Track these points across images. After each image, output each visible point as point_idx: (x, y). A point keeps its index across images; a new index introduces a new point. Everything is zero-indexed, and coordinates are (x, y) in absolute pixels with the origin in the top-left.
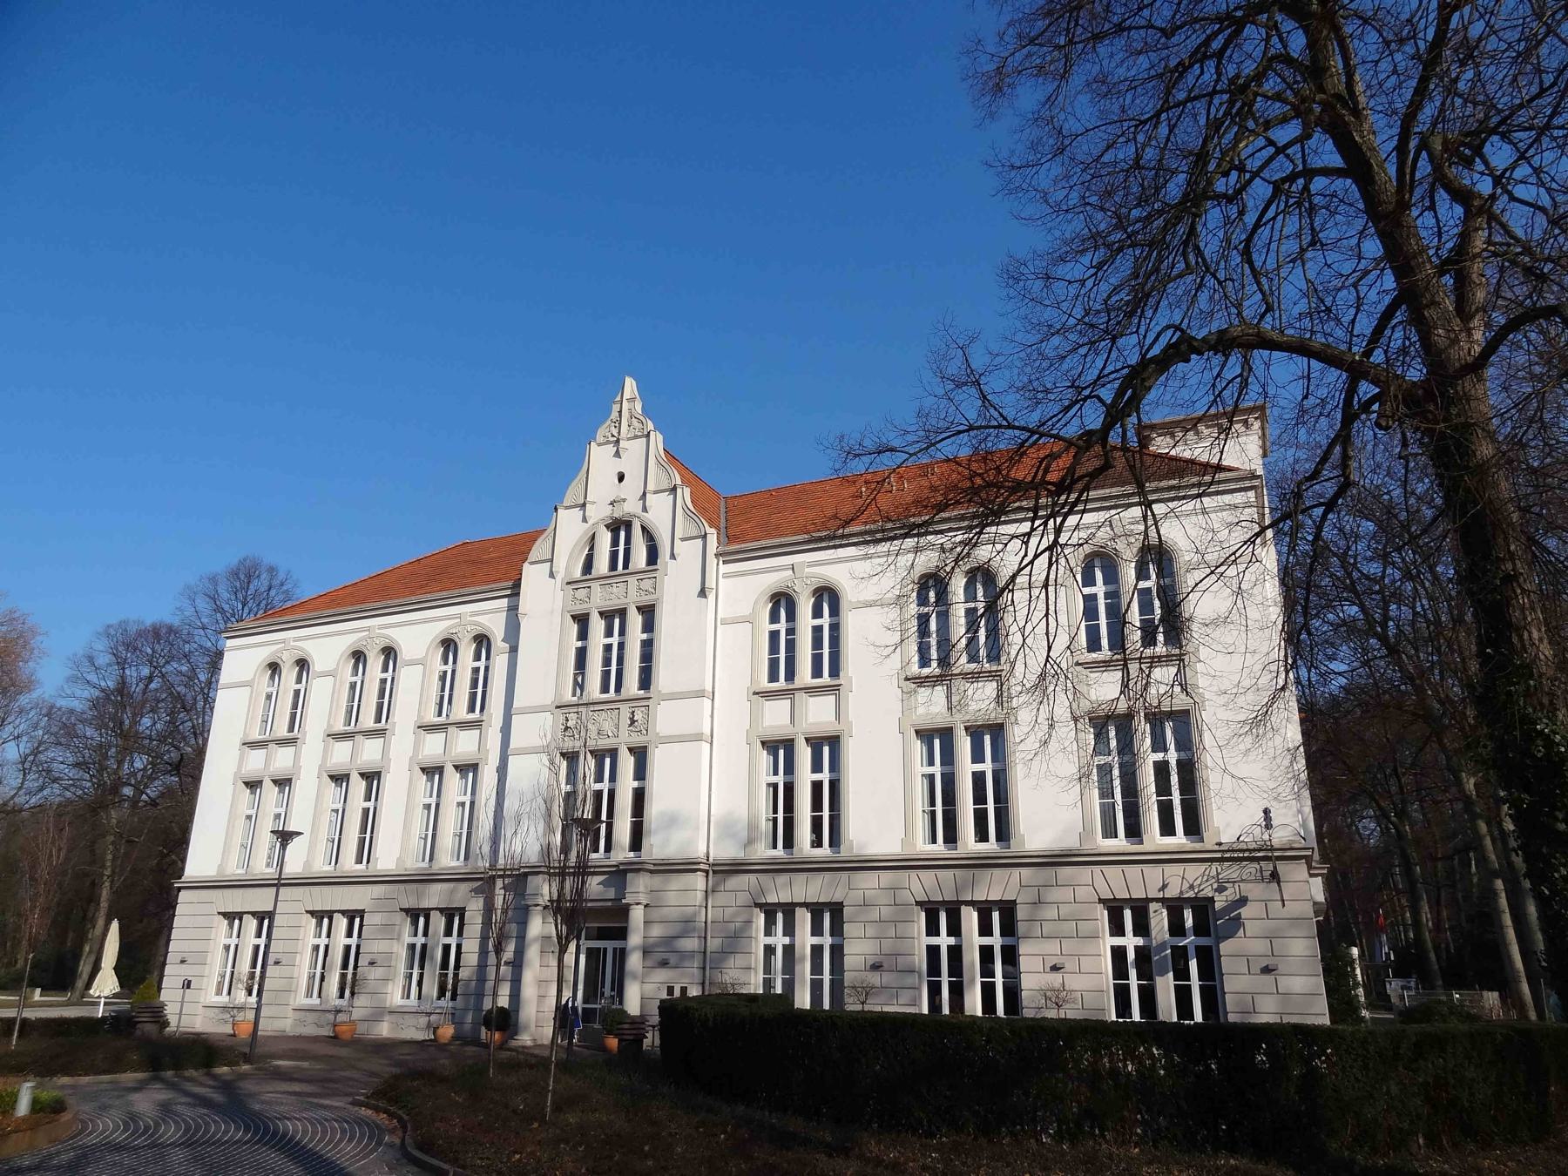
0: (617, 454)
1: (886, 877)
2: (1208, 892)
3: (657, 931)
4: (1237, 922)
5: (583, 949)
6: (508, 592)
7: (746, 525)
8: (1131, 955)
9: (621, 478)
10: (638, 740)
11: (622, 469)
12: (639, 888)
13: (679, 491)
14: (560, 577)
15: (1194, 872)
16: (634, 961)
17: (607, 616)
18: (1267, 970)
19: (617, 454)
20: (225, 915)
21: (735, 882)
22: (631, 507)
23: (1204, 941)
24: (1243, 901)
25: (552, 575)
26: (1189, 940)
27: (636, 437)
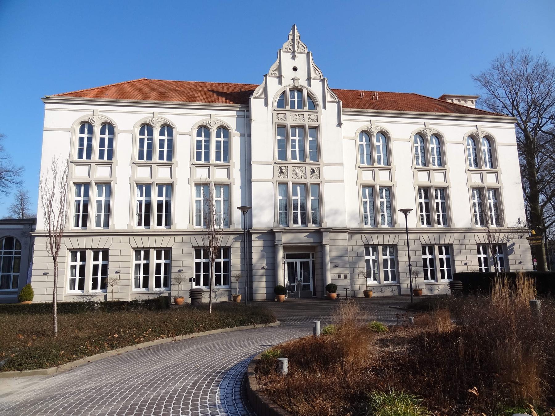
2: (505, 241)
3: (334, 254)
4: (512, 250)
5: (286, 262)
6: (238, 109)
7: (352, 101)
8: (483, 260)
9: (295, 69)
11: (294, 66)
12: (327, 239)
16: (329, 266)
17: (293, 127)
18: (520, 263)
19: (294, 58)
21: (358, 236)
22: (303, 83)
23: (501, 256)
24: (514, 244)
25: (266, 104)
27: (301, 53)
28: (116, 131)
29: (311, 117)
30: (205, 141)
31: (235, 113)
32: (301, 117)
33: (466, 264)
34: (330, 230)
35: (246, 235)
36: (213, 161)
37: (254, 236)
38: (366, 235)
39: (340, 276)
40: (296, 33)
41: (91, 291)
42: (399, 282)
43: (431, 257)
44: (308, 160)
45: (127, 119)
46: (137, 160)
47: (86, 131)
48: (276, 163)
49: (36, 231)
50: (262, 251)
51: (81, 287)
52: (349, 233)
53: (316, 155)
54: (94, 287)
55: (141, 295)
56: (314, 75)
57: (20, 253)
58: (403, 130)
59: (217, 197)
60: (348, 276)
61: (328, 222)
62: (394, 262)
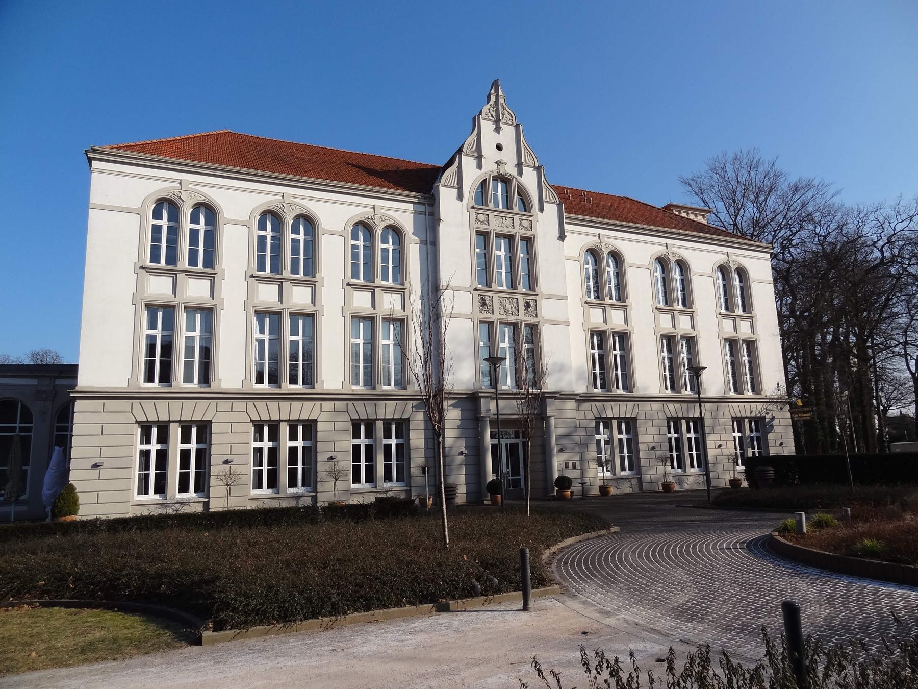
1: (656, 406)
2: (764, 415)
3: (561, 431)
4: (772, 427)
7: (579, 205)
9: (499, 147)
15: (760, 406)
16: (555, 451)
17: (498, 236)
19: (498, 129)
21: (586, 405)
22: (510, 169)
24: (773, 418)
25: (460, 197)
27: (508, 124)
28: (221, 221)
29: (523, 222)
30: (272, 238)
31: (410, 207)
32: (510, 221)
33: (720, 446)
34: (555, 396)
35: (433, 399)
36: (287, 273)
37: (447, 403)
38: (597, 403)
39: (567, 465)
40: (501, 93)
41: (180, 496)
42: (639, 472)
44: (521, 289)
45: (241, 200)
46: (148, 263)
47: (165, 215)
48: (476, 290)
49: (77, 389)
50: (459, 427)
51: (161, 488)
52: (576, 400)
53: (532, 284)
54: (184, 488)
55: (266, 501)
56: (526, 160)
57: (29, 429)
58: (639, 250)
59: (387, 341)
60: (578, 464)
61: (550, 384)
62: (633, 444)
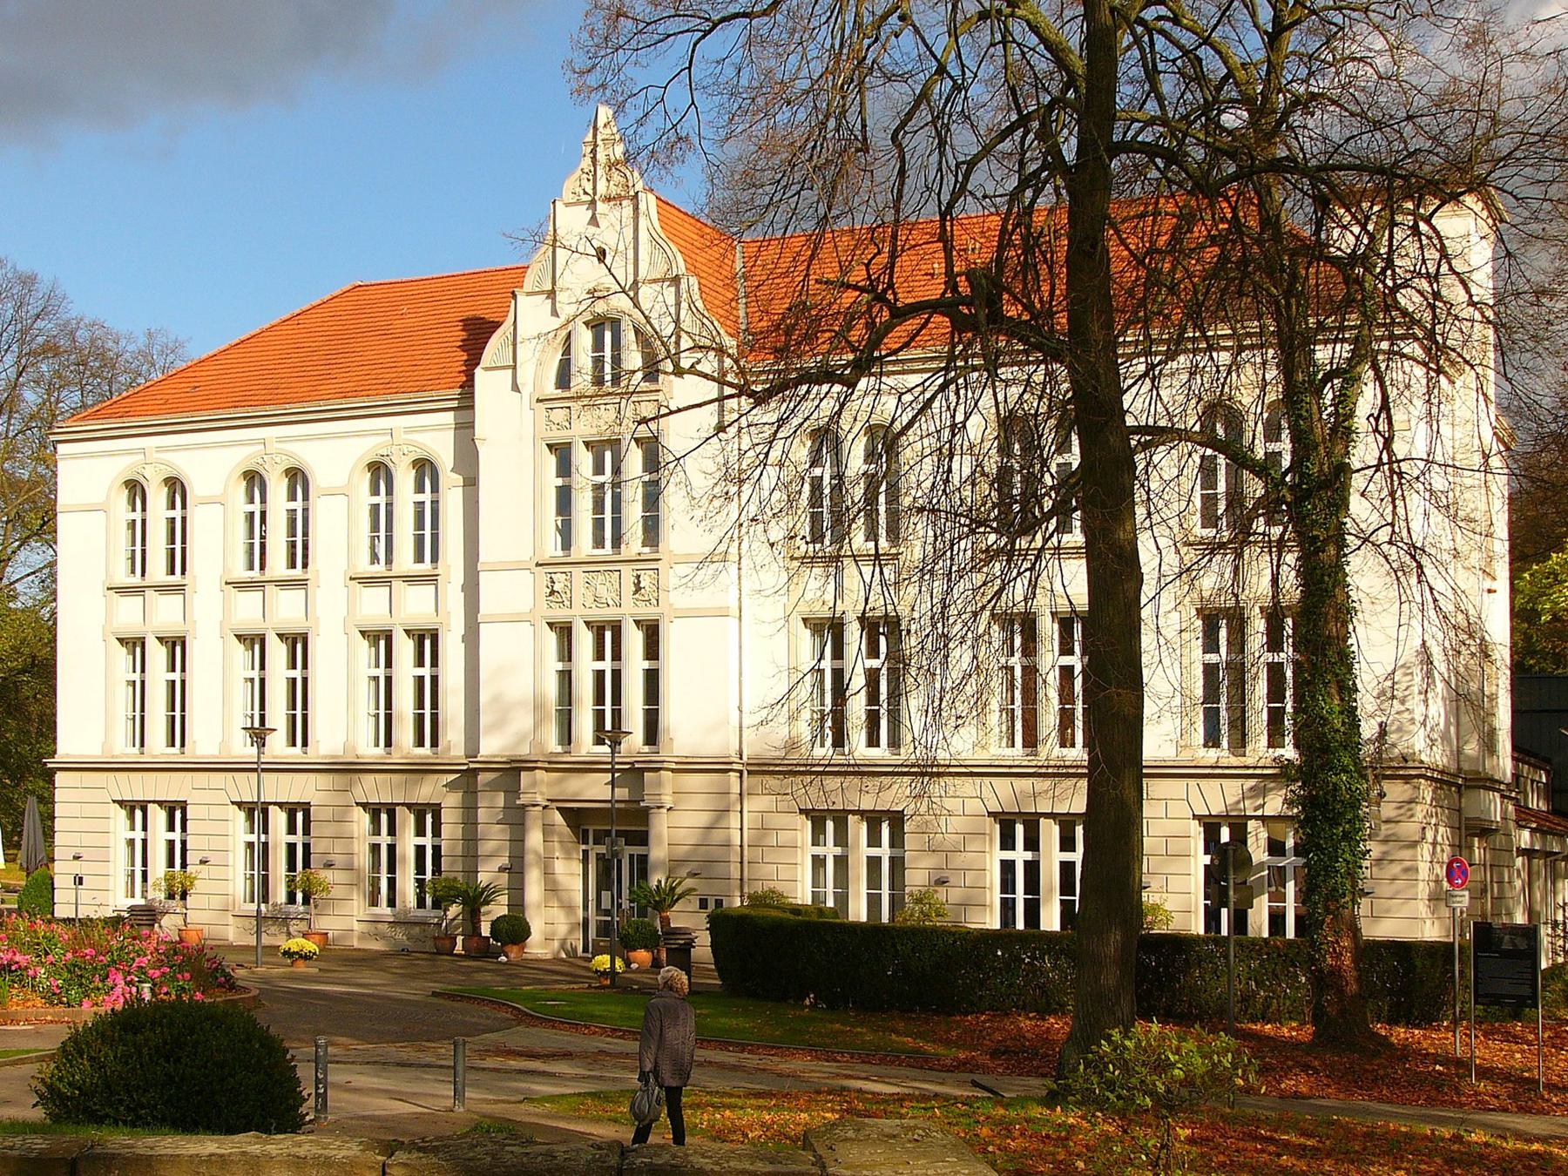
0: (594, 221)
6: (455, 404)
10: (647, 612)
13: (684, 282)
14: (527, 389)
19: (594, 221)
20: (121, 803)
26: (1289, 861)
43: (1029, 856)
